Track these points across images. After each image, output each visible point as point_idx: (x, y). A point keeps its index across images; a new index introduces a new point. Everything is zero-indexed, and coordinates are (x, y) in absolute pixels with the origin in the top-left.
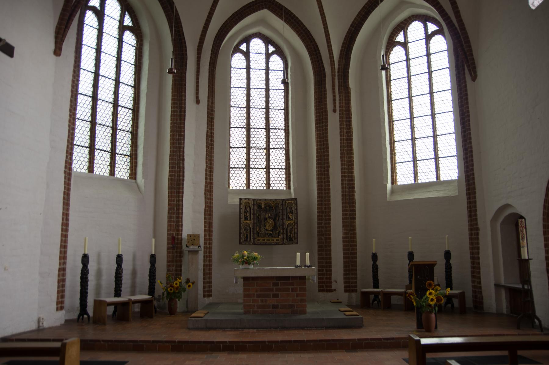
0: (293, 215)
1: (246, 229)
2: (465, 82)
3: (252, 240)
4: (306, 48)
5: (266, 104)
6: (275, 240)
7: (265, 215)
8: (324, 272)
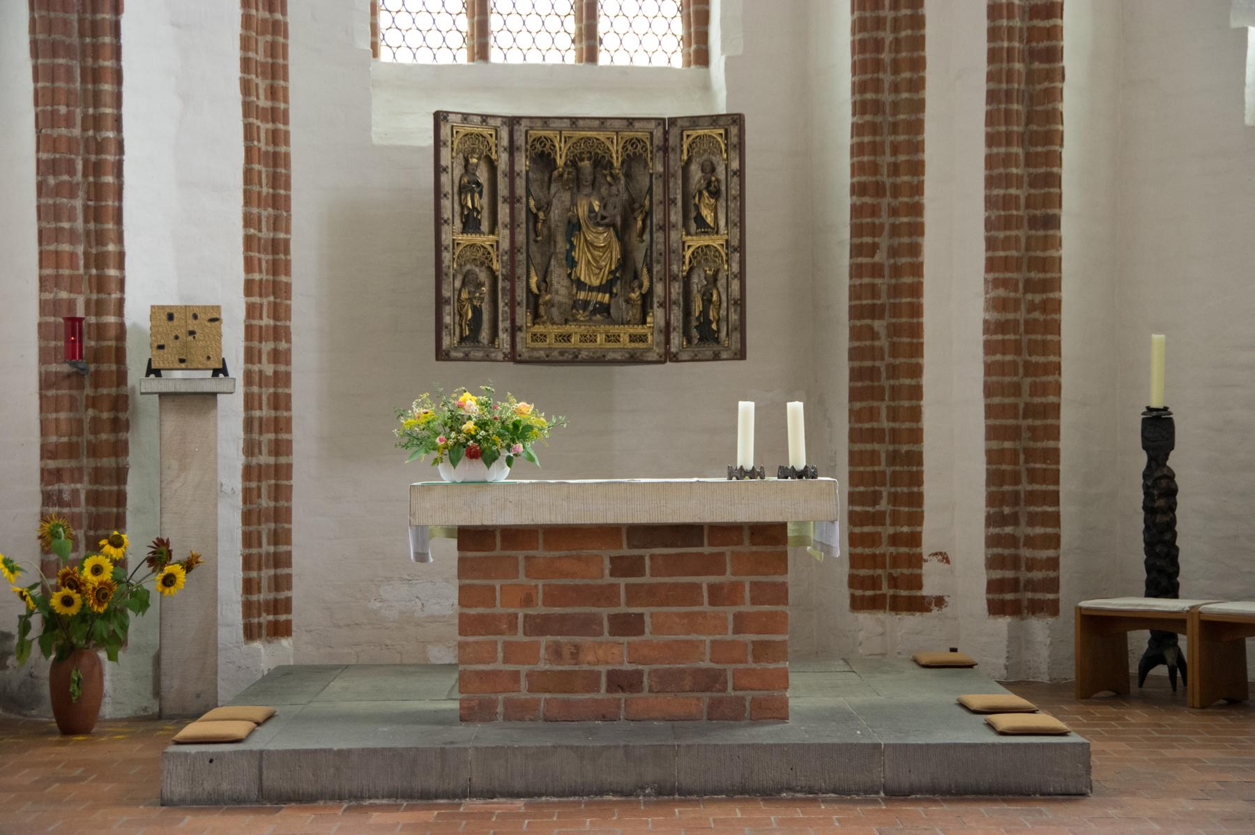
0: (722, 202)
1: (469, 280)
3: (504, 337)
6: (625, 338)
7: (574, 204)
8: (884, 505)
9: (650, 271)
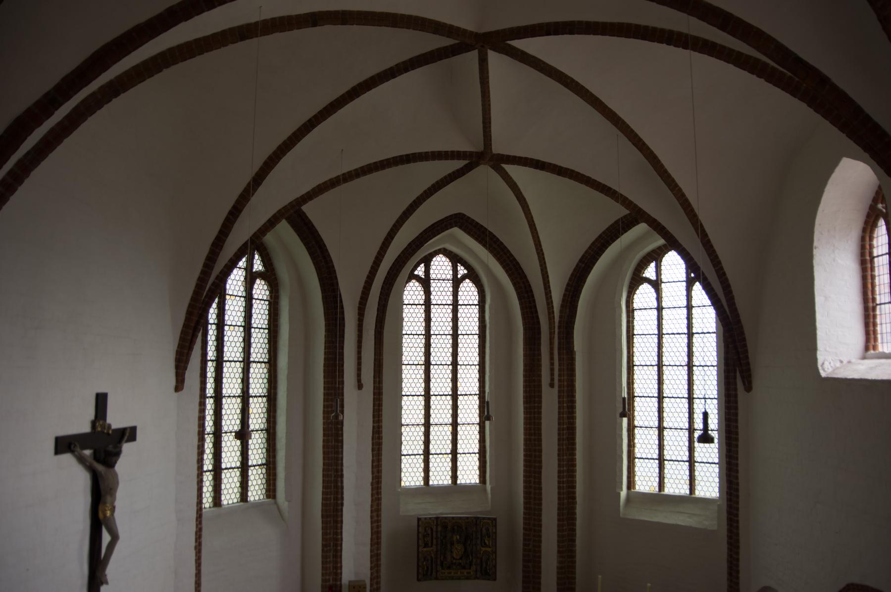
2: (736, 390)
3: (434, 573)
4: (514, 286)
5: (453, 359)
6: (465, 573)
9: (472, 555)
